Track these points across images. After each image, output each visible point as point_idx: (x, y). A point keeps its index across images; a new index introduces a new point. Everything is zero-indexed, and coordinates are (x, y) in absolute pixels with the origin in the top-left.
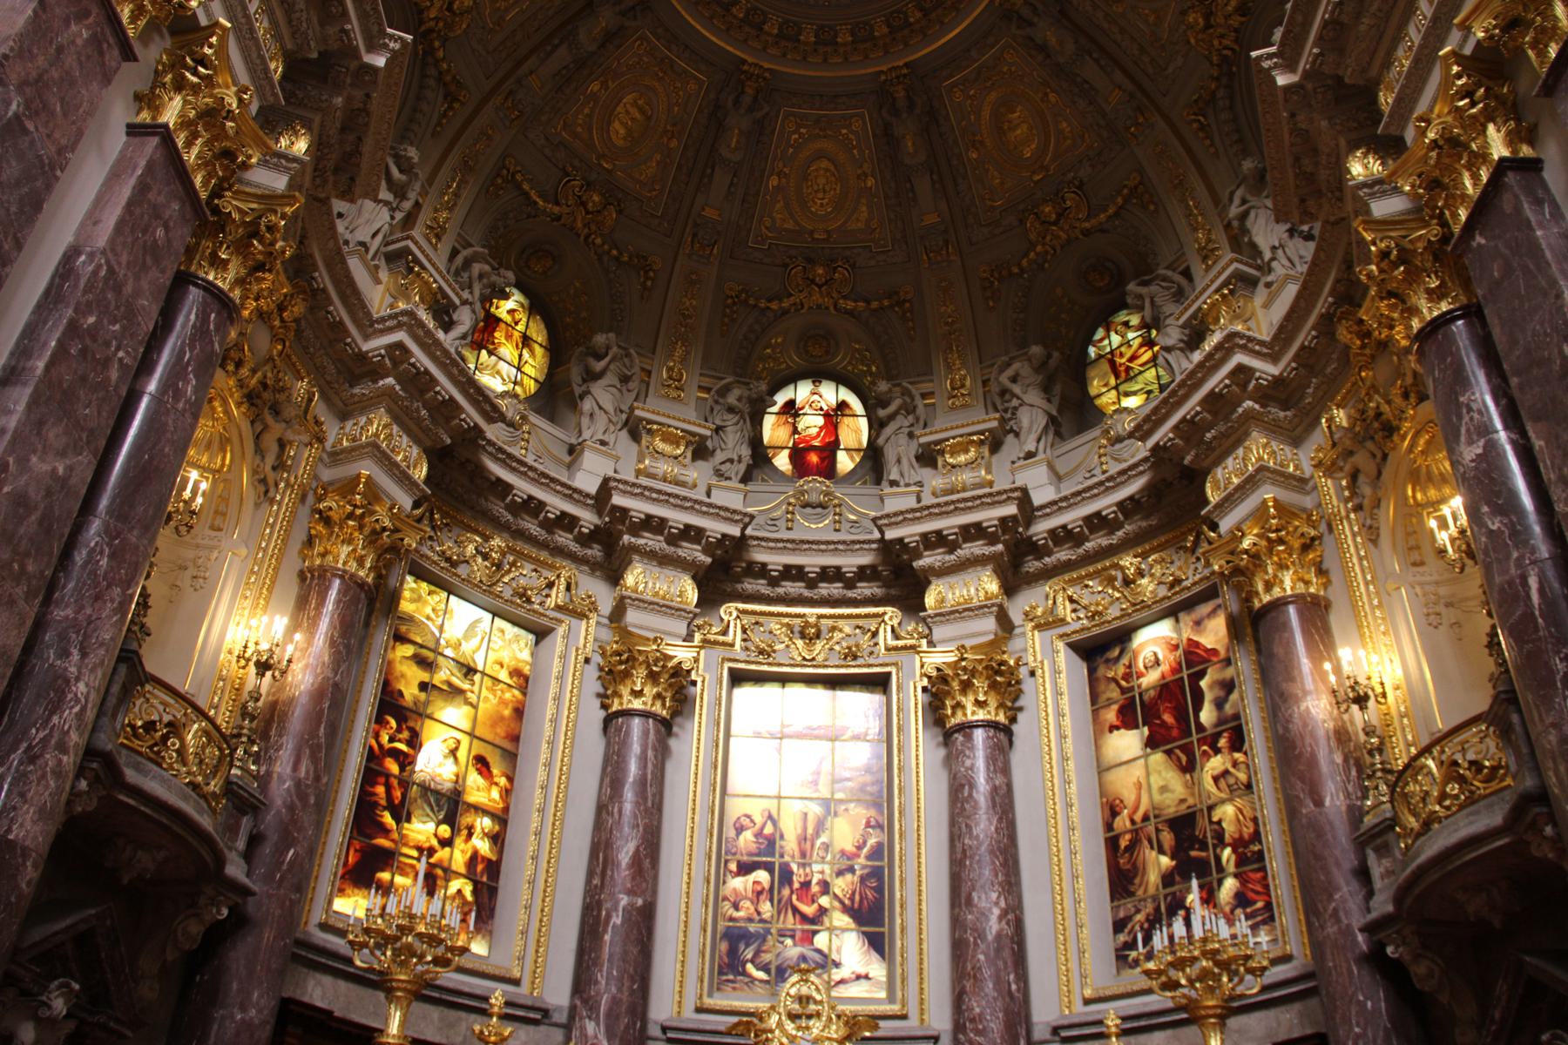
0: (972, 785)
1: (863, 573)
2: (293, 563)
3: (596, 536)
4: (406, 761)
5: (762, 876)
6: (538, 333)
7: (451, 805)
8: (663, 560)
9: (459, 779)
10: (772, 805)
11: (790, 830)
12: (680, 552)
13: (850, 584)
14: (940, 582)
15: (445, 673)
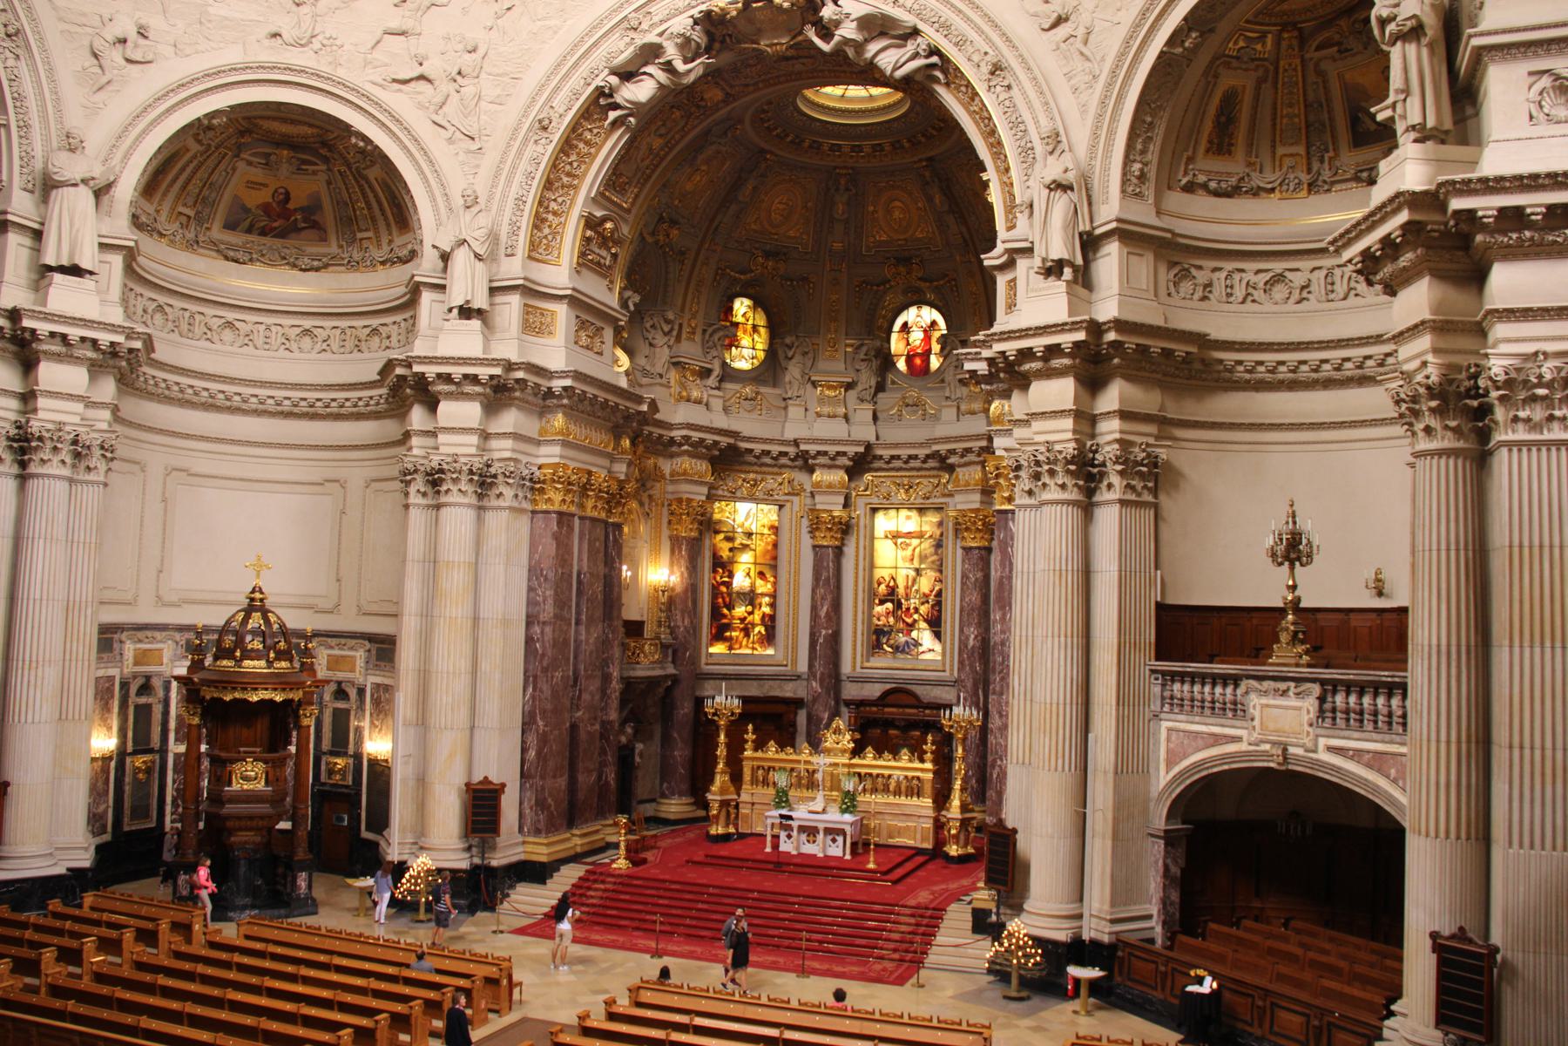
0: (968, 578)
1: (928, 457)
2: (666, 533)
3: (797, 456)
4: (728, 585)
5: (889, 605)
6: (761, 320)
7: (751, 597)
8: (830, 467)
9: (753, 585)
10: (892, 571)
11: (901, 583)
12: (837, 463)
13: (924, 462)
14: (958, 470)
15: (740, 540)
